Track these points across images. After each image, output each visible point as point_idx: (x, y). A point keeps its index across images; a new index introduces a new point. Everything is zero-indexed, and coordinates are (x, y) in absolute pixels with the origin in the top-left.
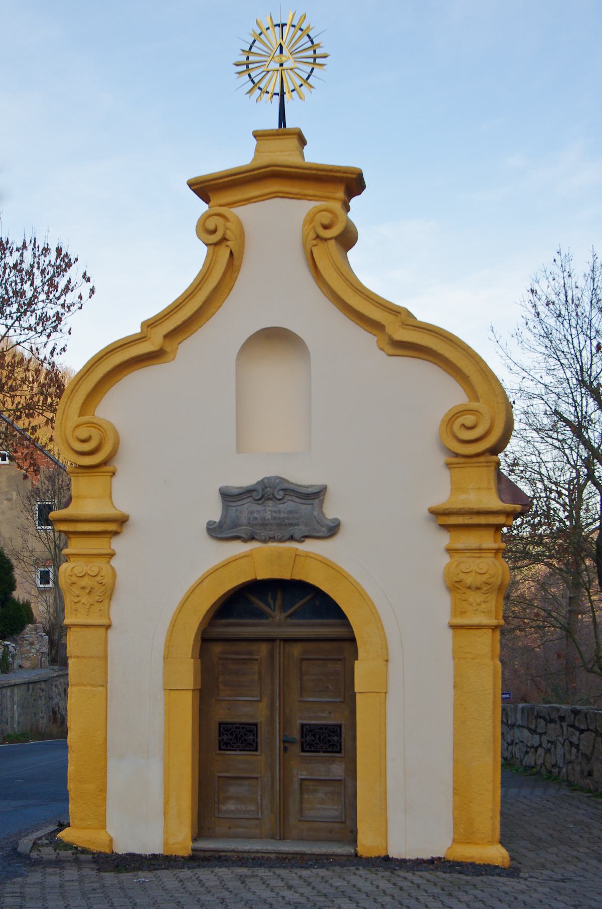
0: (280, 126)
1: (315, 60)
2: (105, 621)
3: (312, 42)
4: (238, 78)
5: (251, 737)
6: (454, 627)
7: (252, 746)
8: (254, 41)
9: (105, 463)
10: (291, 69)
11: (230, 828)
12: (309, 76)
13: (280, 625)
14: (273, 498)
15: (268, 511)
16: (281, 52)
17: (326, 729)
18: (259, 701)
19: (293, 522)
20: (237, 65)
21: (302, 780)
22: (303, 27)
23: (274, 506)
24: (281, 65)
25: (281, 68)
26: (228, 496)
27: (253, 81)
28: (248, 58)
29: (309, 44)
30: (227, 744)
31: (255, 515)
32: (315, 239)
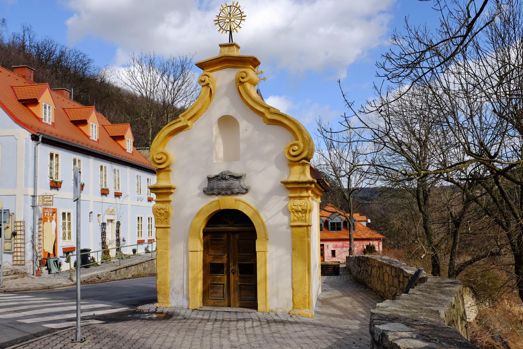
0: (230, 42)
14: (225, 179)
15: (224, 184)
16: (230, 16)
20: (215, 21)
22: (237, 6)
24: (230, 20)
26: (210, 179)
29: (240, 12)
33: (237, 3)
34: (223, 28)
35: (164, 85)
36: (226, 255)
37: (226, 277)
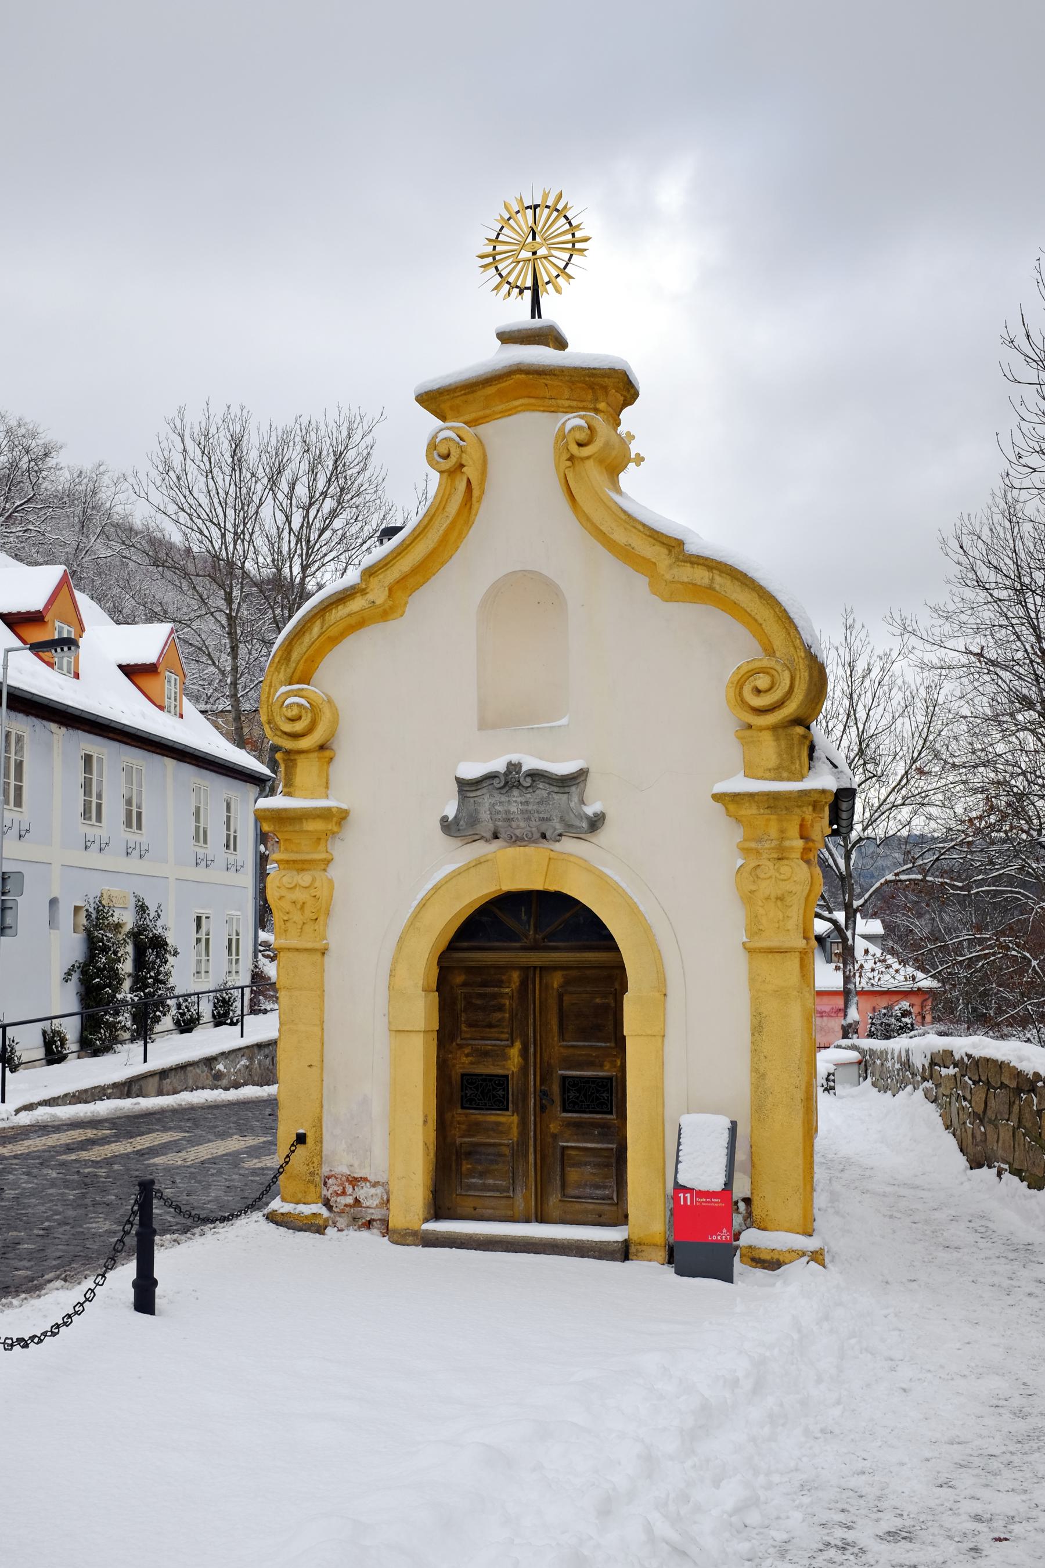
1: (574, 245)
2: (318, 945)
3: (570, 223)
4: (484, 271)
5: (501, 1093)
6: (750, 951)
7: (501, 1105)
8: (502, 227)
9: (322, 747)
10: (545, 258)
11: (475, 1209)
12: (567, 264)
13: (535, 948)
14: (518, 785)
16: (534, 238)
17: (593, 1082)
18: (512, 1045)
19: (545, 816)
20: (482, 257)
21: (564, 1148)
22: (560, 207)
23: (521, 796)
24: (534, 253)
25: (535, 257)
26: (466, 787)
27: (500, 275)
28: (494, 248)
29: (567, 226)
30: (471, 1101)
31: (498, 808)
32: (568, 460)
33: (560, 196)
34: (511, 279)
35: (281, 518)
36: (518, 1045)
37: (515, 1119)
